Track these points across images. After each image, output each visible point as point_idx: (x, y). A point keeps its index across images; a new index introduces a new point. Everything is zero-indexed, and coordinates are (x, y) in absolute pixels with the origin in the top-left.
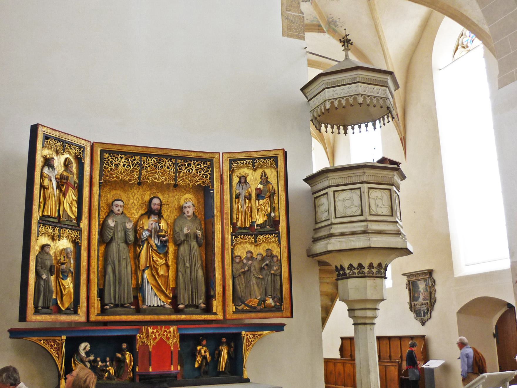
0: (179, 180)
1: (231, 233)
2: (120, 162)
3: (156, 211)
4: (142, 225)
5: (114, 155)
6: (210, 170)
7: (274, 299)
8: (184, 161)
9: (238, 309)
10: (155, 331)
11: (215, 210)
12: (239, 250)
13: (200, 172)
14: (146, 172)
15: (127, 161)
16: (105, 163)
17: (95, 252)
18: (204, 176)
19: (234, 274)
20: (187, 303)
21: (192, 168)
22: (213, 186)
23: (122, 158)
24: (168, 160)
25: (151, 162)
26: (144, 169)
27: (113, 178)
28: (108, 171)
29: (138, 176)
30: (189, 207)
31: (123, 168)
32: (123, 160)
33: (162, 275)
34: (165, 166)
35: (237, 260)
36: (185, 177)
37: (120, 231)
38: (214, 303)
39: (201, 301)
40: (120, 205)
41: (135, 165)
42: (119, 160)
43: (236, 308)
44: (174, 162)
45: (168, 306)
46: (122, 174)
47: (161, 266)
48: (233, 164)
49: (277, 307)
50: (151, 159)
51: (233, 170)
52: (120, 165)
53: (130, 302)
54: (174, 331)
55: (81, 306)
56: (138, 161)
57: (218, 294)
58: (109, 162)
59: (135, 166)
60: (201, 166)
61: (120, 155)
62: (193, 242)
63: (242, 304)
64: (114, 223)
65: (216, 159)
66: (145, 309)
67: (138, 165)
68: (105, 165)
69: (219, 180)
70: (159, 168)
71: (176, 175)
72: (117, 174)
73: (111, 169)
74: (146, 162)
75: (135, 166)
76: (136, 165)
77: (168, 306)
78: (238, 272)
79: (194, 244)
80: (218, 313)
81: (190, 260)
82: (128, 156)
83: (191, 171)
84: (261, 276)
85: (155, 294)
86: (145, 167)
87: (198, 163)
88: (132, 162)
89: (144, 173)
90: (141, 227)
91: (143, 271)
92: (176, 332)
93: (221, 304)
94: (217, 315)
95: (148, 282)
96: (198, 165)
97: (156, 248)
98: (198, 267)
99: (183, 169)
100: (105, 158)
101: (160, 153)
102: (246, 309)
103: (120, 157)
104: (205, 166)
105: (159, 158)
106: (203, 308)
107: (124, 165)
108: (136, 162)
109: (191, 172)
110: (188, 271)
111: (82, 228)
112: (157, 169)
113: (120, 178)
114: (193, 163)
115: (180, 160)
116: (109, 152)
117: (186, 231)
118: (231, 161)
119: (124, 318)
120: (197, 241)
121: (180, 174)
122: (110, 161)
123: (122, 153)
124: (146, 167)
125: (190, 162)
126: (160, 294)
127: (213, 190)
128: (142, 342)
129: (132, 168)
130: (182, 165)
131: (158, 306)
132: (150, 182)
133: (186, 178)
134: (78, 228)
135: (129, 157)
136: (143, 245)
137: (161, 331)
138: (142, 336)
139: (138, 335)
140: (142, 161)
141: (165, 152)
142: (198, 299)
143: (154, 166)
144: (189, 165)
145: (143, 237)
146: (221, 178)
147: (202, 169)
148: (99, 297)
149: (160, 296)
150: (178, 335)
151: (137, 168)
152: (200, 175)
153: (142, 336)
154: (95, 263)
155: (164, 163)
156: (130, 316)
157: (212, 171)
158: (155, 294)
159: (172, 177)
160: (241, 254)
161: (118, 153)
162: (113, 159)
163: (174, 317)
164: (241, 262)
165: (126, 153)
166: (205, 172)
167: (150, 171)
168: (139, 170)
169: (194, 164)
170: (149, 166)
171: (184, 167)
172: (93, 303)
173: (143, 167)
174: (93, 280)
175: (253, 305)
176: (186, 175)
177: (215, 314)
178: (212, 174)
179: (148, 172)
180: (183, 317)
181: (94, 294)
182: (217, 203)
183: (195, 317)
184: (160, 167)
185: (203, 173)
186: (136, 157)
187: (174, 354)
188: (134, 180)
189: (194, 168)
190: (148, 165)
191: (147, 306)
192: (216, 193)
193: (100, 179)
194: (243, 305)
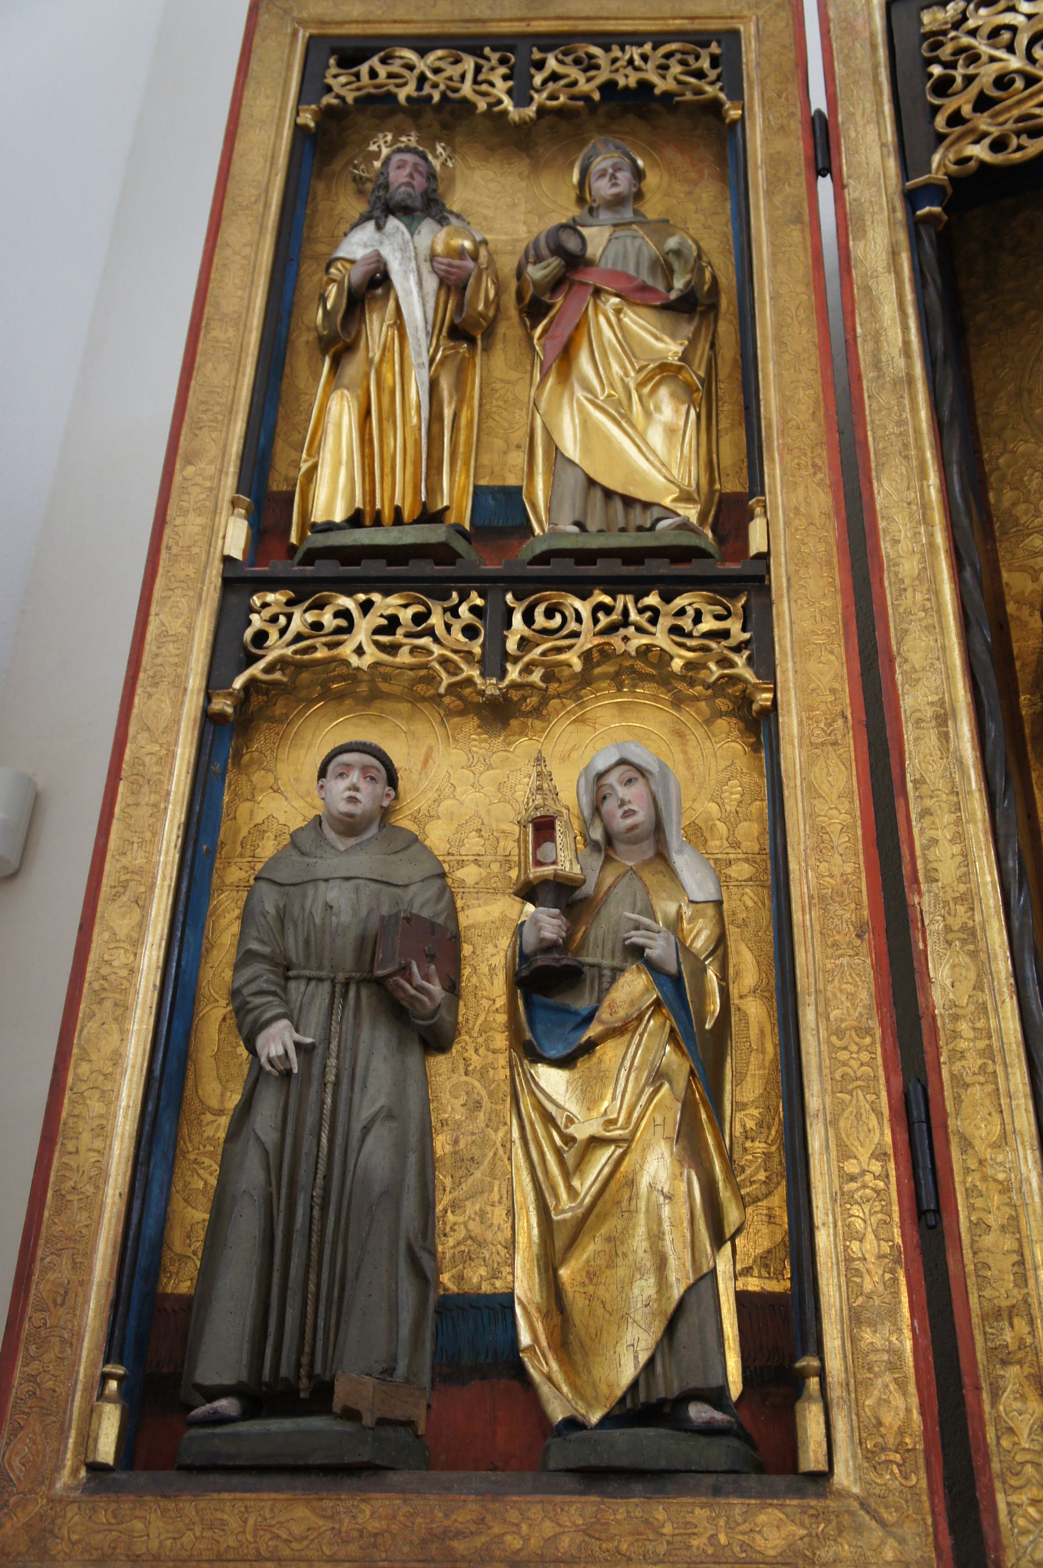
17: (944, 737)
55: (834, 1364)
73: (1003, 82)
154: (959, 837)
172: (996, 1314)
174: (964, 1027)
181: (1005, 1188)
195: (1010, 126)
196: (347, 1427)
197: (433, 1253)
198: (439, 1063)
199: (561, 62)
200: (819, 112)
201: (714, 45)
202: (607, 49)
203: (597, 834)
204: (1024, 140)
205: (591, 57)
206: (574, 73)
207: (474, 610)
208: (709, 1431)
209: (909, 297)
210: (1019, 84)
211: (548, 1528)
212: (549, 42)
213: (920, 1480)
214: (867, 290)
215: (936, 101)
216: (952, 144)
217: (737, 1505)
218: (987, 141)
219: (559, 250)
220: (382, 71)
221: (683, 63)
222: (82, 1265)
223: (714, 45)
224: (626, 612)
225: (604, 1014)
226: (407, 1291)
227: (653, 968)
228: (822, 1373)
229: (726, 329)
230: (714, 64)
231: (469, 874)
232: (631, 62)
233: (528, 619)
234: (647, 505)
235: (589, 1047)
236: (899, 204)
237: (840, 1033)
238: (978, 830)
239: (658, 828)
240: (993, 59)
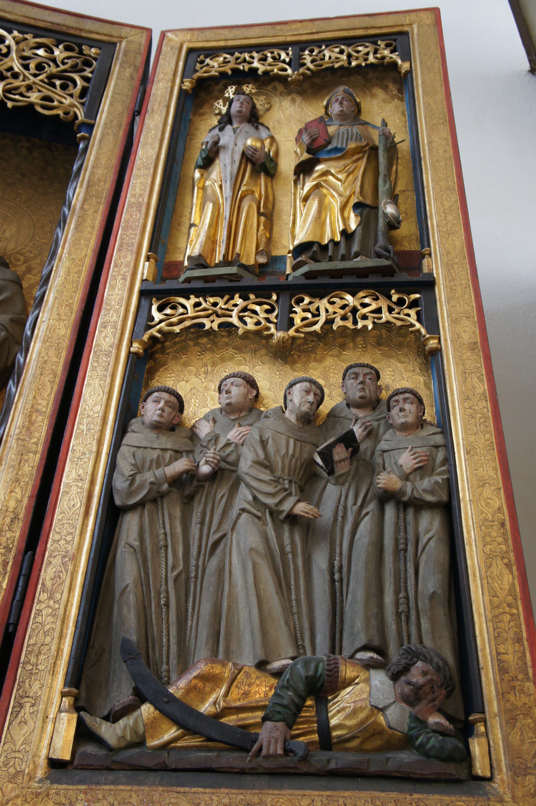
1: (143, 281)
7: (406, 669)
9: (100, 741)
18: (58, 83)
19: (120, 483)
48: (202, 62)
49: (434, 741)
63: (143, 700)
65: (127, 41)
78: (149, 476)
84: (302, 508)
96: (39, 46)
102: (165, 746)
127: (90, 127)
175: (227, 710)
192: (103, 135)
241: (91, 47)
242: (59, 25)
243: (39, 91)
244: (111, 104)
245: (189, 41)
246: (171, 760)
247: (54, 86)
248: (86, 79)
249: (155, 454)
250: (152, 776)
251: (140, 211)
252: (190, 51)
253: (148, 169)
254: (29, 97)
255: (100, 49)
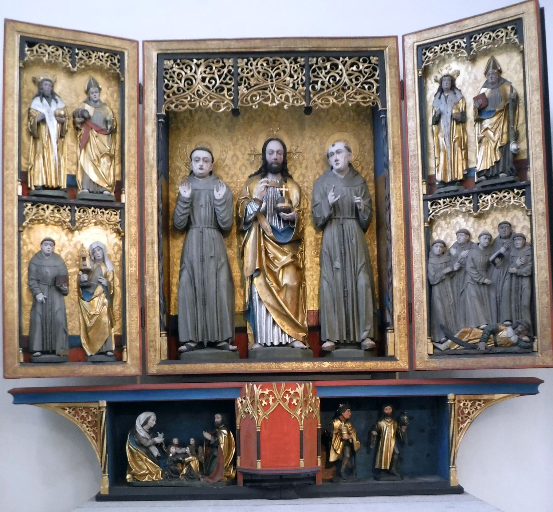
0: (315, 98)
2: (195, 72)
3: (274, 166)
4: (248, 194)
5: (183, 61)
6: (377, 73)
8: (324, 61)
10: (267, 392)
11: (390, 152)
12: (441, 231)
13: (357, 79)
14: (248, 89)
15: (208, 70)
16: (166, 78)
17: (153, 247)
18: (366, 87)
19: (431, 278)
20: (337, 338)
21: (340, 73)
22: (384, 104)
23: (198, 66)
24: (290, 60)
25: (256, 68)
26: (243, 82)
27: (184, 106)
28: (174, 93)
29: (232, 98)
30: (338, 152)
31: (203, 84)
32: (202, 69)
33: (286, 285)
34: (284, 72)
35: (437, 249)
36: (326, 91)
37: (204, 206)
38: (390, 336)
39: (365, 334)
40: (204, 159)
41: (224, 76)
42: (193, 71)
43: (434, 347)
44: (302, 63)
45: (299, 345)
46: (200, 96)
47: (283, 267)
48: (425, 54)
50: (256, 61)
51: (425, 67)
52: (195, 79)
53: (225, 338)
54: (305, 391)
56: (230, 68)
57: (399, 320)
58: (175, 76)
59: (225, 79)
60: (358, 67)
61: (195, 61)
62: (349, 220)
63: (448, 339)
64: (190, 191)
65: (389, 49)
66: (256, 351)
67: (232, 75)
68: (166, 81)
69: (397, 91)
70: (272, 77)
71: (308, 88)
72: (191, 98)
74: (247, 69)
75: (225, 79)
76: (226, 76)
77: (299, 345)
78: (439, 275)
79: (351, 225)
80: (398, 358)
81: (343, 255)
82: (210, 60)
83: (338, 78)
85: (274, 322)
86: (244, 78)
87: (352, 60)
88: (219, 71)
89: (242, 89)
90: (246, 198)
91: (252, 278)
92: (310, 395)
93: (405, 339)
94: (397, 360)
95: (260, 299)
96: (352, 65)
97: (272, 234)
98: (359, 268)
99: (321, 75)
100: (165, 69)
101: (273, 49)
102: (455, 349)
103: (196, 64)
104: (366, 65)
105: (271, 60)
106: (368, 348)
107: (203, 79)
108: (226, 70)
109: (338, 79)
110: (339, 275)
111: (124, 204)
112: (269, 80)
113: (198, 104)
114: (342, 62)
115: (315, 59)
116: (174, 56)
117: (331, 198)
118: (422, 49)
119: (211, 368)
120: (357, 218)
121: (316, 87)
122: (176, 74)
123: (199, 57)
124: (247, 78)
125: (336, 61)
126: (282, 321)
127: (385, 112)
128: (245, 412)
129: (218, 82)
130: (320, 68)
131: (281, 344)
132: (257, 106)
133: (329, 94)
134: (117, 205)
135: (213, 63)
136: (250, 230)
137: (279, 391)
138: (244, 401)
139: (239, 400)
140: (239, 67)
141: (281, 46)
142: (359, 331)
143: (263, 75)
144: (335, 66)
145: (247, 215)
146: (402, 86)
147: (360, 72)
148: (165, 330)
149: (283, 326)
150: (316, 400)
151: (229, 82)
152: (357, 85)
153: (244, 401)
154: (153, 266)
155: (282, 67)
156: (223, 364)
157: (383, 74)
158: (274, 322)
159: (300, 94)
160: (446, 238)
161: (190, 56)
162: (182, 69)
163: (307, 366)
164: (447, 254)
165: (207, 56)
166: (367, 78)
167: (255, 85)
168: (233, 86)
169: (344, 65)
170: (253, 76)
171: (323, 71)
173: (241, 79)
174: (151, 299)
175: (469, 340)
176: (328, 88)
177: (393, 358)
178: (382, 82)
179: (251, 87)
180: (326, 365)
181: (154, 324)
182: (393, 137)
183: (350, 365)
184: (274, 76)
185: (362, 79)
186: (225, 61)
187: (306, 436)
188: (224, 106)
189: (344, 71)
190: (251, 74)
191: (260, 344)
192: (392, 117)
193: (159, 108)
194: (449, 341)
195: (178, 102)
196: (58, 357)
197: (67, 329)
198: (66, 298)
199: (83, 55)
200: (140, 84)
201: (118, 56)
202: (94, 52)
203: (93, 258)
204: (181, 107)
205: (90, 54)
206: (85, 58)
207: (69, 210)
208: (111, 356)
209: (155, 144)
210: (182, 91)
211: (89, 369)
212: (80, 47)
213: (139, 362)
214: (147, 140)
215: (165, 90)
216: (167, 103)
217: (114, 366)
218: (174, 105)
219: (83, 117)
220: (39, 51)
221: (111, 60)
222: (13, 333)
223: (118, 56)
224: (98, 213)
225: (95, 294)
226: (64, 335)
227: (103, 285)
228: (126, 348)
229: (118, 136)
230: (118, 62)
231: (69, 262)
232: (99, 57)
233: (79, 212)
234: (101, 187)
235: (93, 299)
236: (156, 118)
237: (132, 298)
238: (156, 265)
239: (104, 258)
240: (177, 83)
241: (374, 56)
242: (358, 47)
243: (360, 94)
244: (391, 97)
245: (417, 42)
246: (457, 352)
247: (364, 88)
248: (376, 81)
249: (439, 266)
250: (454, 356)
251: (415, 159)
252: (418, 46)
253: (414, 134)
254: (356, 99)
255: (378, 56)
